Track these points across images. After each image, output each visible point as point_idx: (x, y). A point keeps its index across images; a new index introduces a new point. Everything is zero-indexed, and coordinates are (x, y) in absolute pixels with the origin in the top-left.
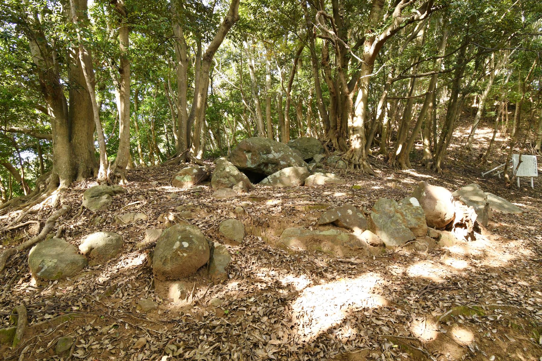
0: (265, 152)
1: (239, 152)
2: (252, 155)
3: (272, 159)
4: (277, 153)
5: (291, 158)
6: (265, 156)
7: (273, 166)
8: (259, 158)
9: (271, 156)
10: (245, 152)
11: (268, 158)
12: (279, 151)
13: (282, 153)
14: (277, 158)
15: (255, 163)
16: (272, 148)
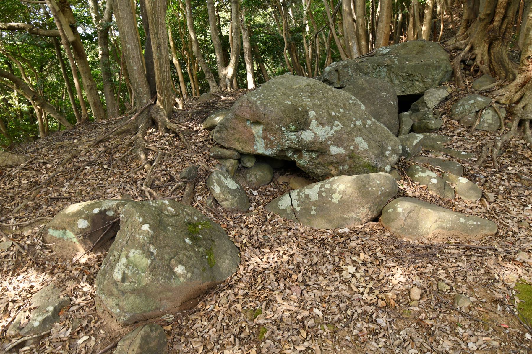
0: (293, 128)
1: (237, 122)
2: (264, 130)
3: (311, 142)
4: (323, 125)
5: (359, 139)
6: (293, 136)
7: (314, 155)
8: (280, 138)
9: (307, 136)
10: (248, 124)
11: (300, 141)
12: (330, 121)
13: (338, 126)
14: (322, 139)
15: (272, 146)
16: (312, 113)
